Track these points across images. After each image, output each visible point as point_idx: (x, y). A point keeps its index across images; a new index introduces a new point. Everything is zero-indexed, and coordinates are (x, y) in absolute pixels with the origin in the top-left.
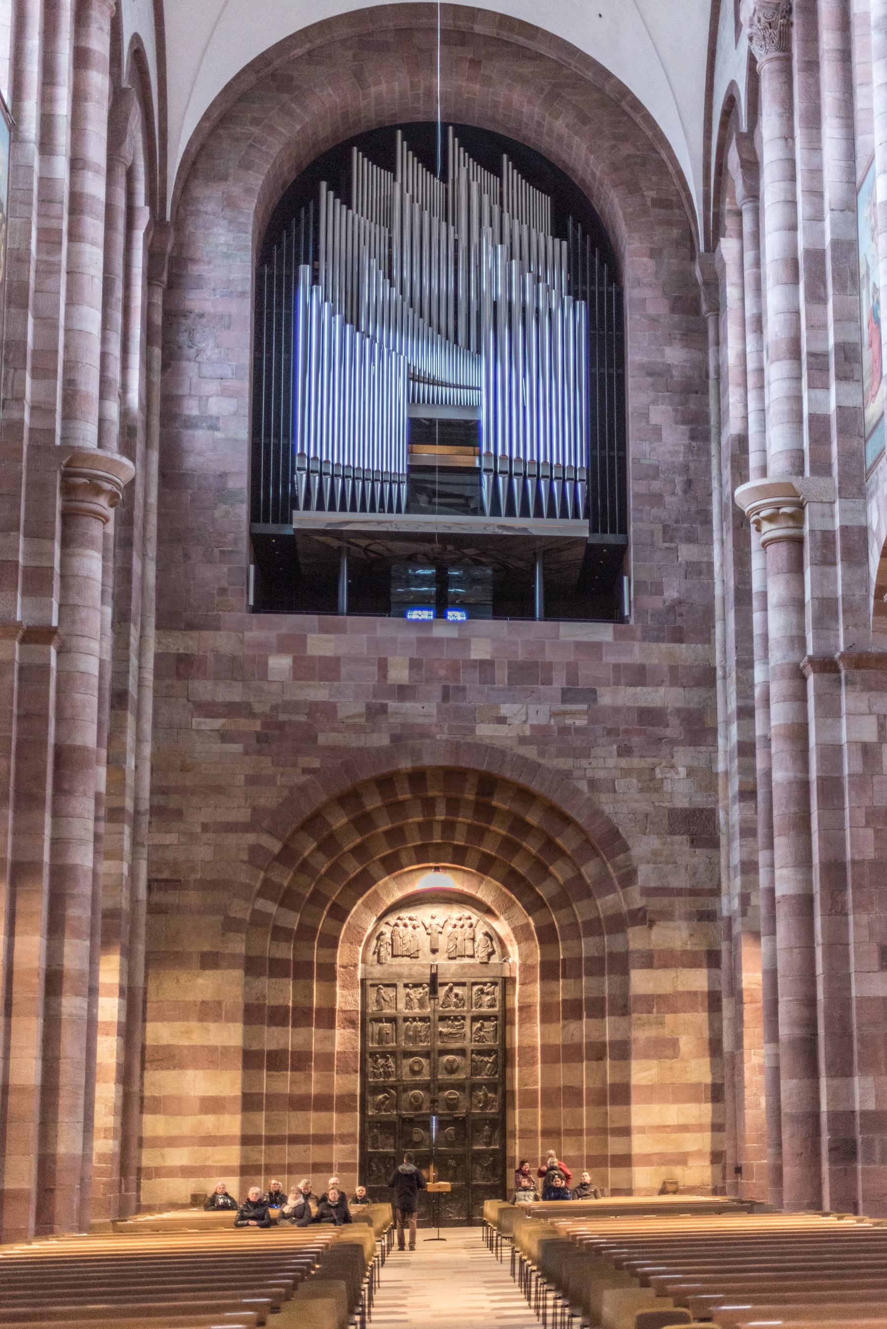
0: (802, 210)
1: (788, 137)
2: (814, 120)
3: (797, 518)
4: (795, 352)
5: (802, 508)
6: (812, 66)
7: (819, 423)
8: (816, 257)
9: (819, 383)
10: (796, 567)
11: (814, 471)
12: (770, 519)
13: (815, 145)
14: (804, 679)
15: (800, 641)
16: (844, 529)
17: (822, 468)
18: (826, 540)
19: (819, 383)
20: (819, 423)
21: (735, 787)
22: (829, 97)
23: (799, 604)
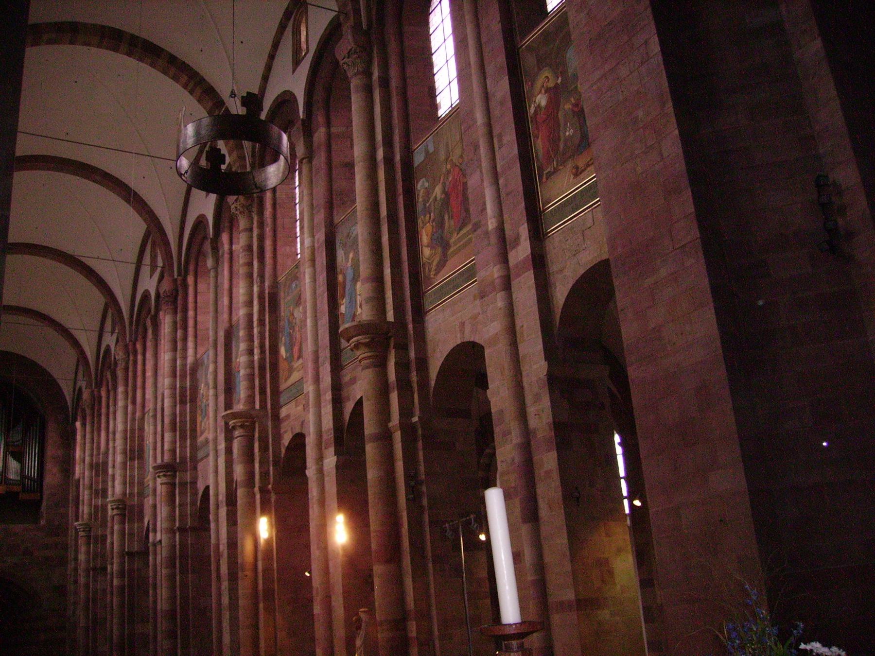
0: (95, 452)
1: (92, 432)
2: (99, 431)
3: (90, 531)
4: (91, 487)
5: (91, 528)
6: (100, 415)
7: (96, 507)
8: (97, 464)
9: (97, 497)
10: (88, 544)
11: (95, 520)
12: (83, 531)
13: (99, 436)
14: (89, 572)
15: (88, 561)
16: (102, 536)
17: (96, 519)
18: (96, 537)
19: (97, 497)
20: (96, 507)
21: (72, 579)
22: (103, 425)
23: (88, 552)
